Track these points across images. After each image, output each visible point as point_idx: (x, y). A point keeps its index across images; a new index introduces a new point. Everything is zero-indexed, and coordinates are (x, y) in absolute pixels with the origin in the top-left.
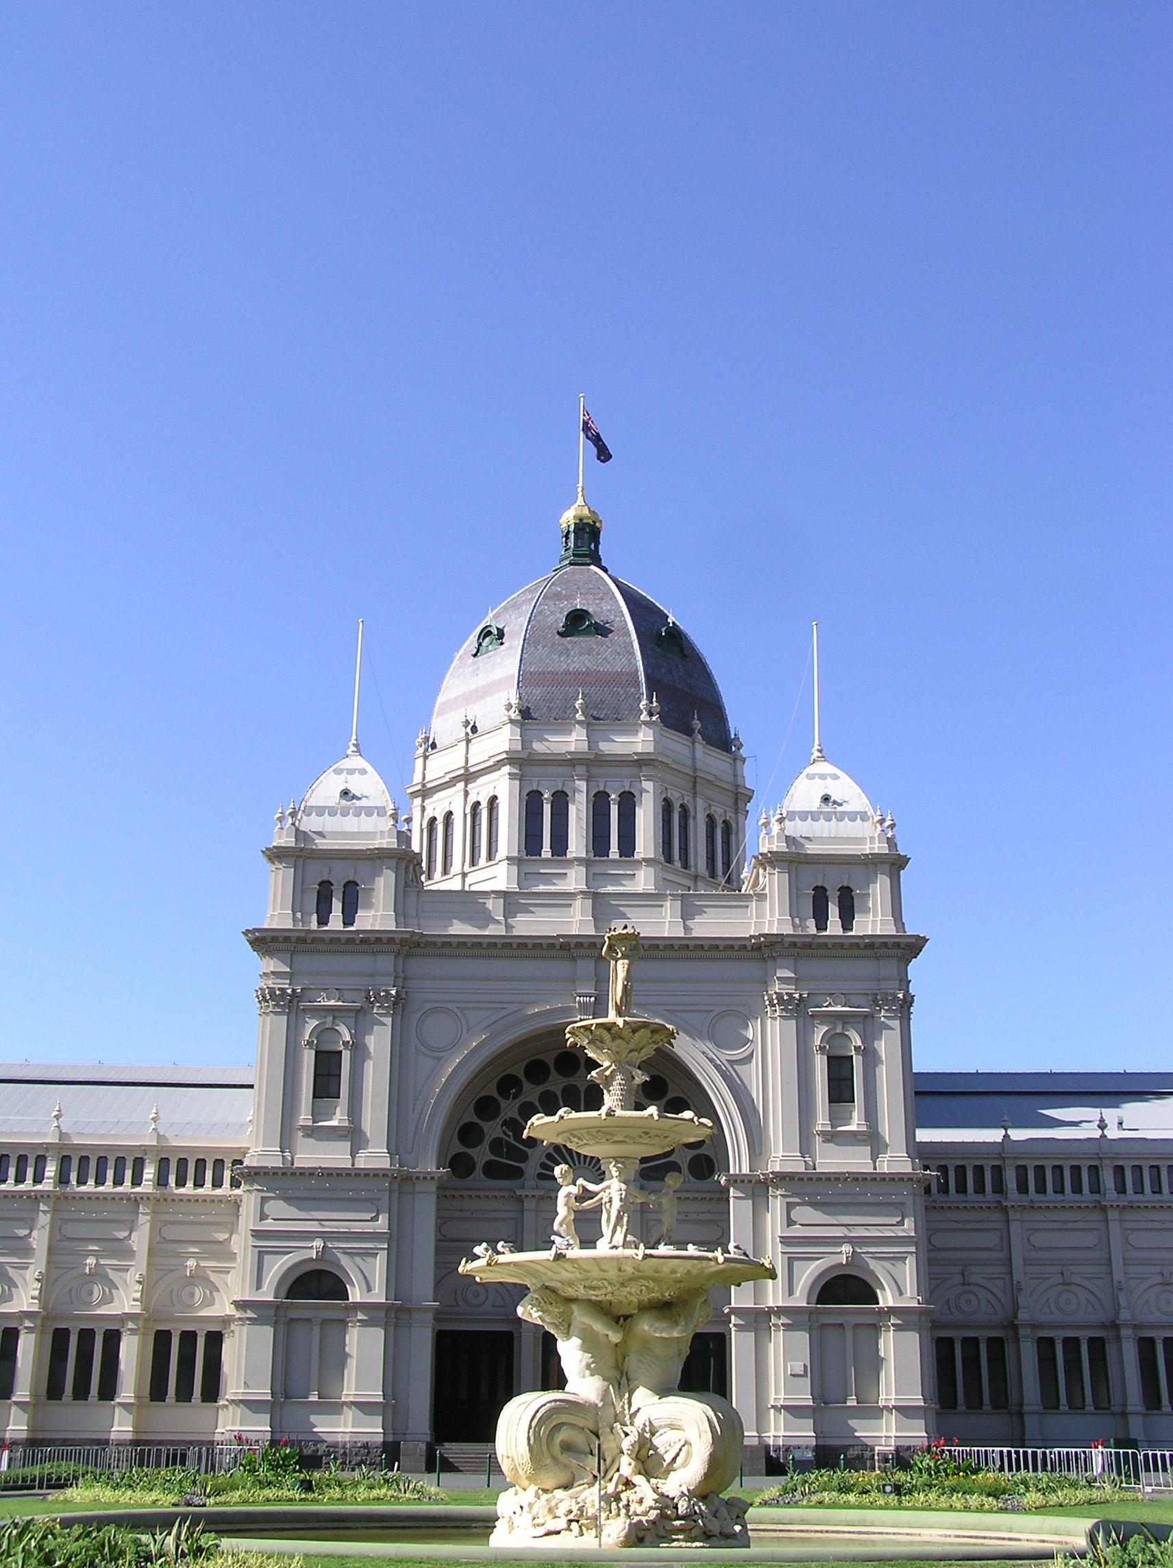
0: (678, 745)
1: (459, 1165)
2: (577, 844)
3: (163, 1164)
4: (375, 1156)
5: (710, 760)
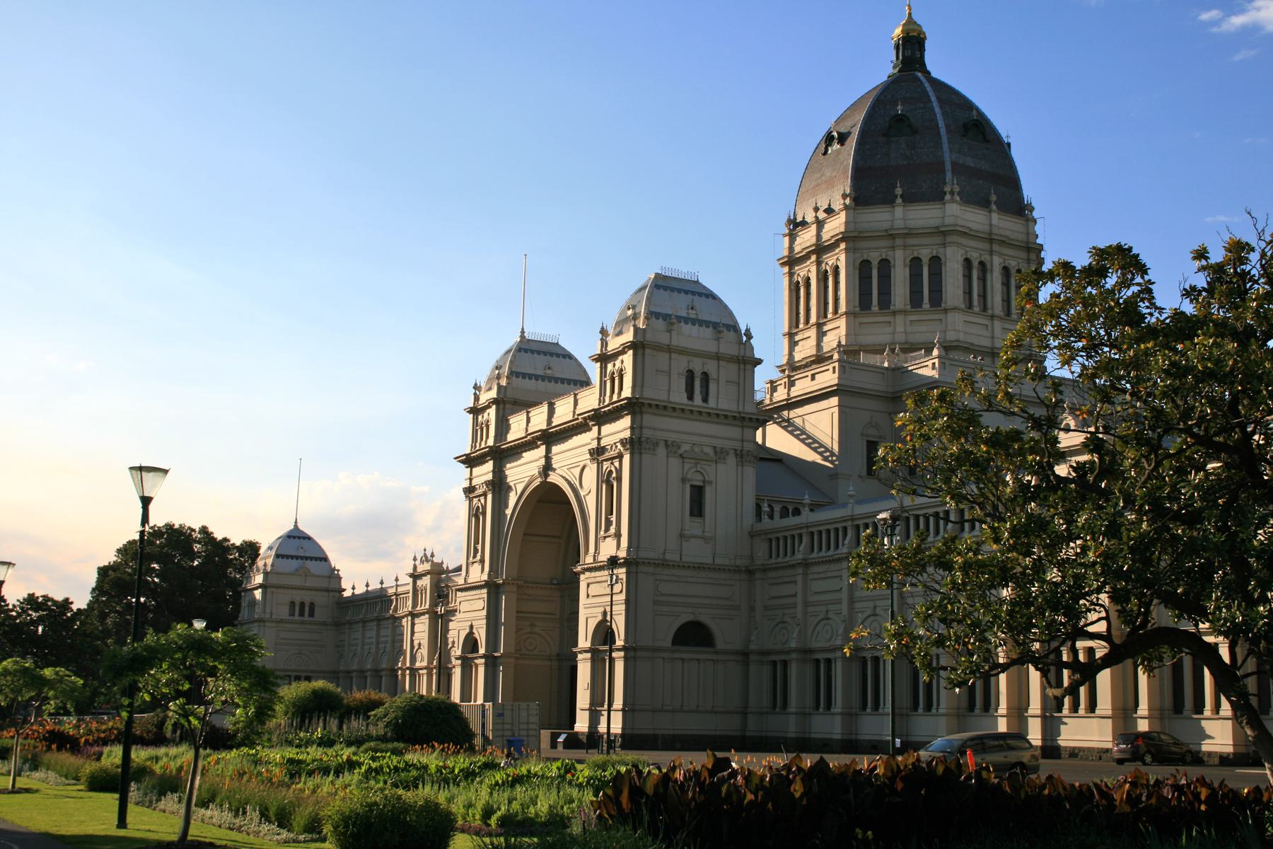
0: (974, 218)
5: (1003, 224)
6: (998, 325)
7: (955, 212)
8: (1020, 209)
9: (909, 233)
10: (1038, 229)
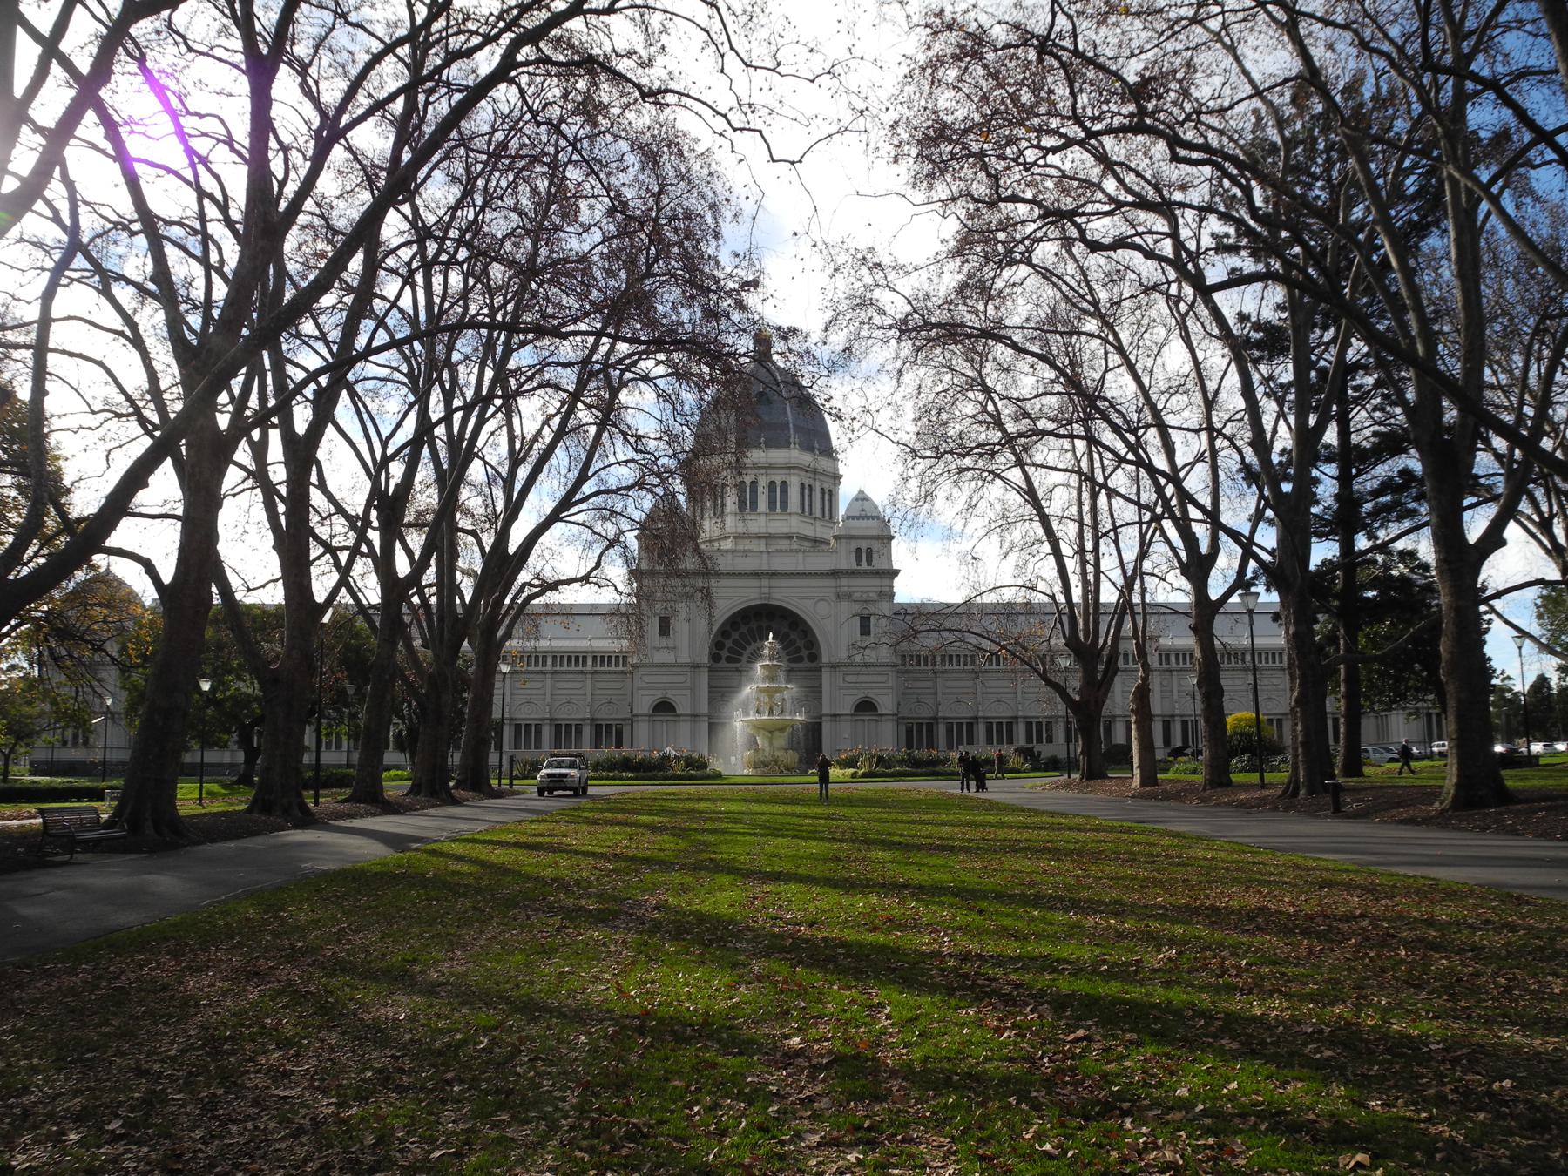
0: (806, 458)
1: (715, 658)
2: (763, 504)
3: (595, 658)
4: (685, 659)
5: (823, 463)
6: (818, 523)
7: (795, 455)
8: (829, 452)
9: (771, 467)
10: (840, 465)
